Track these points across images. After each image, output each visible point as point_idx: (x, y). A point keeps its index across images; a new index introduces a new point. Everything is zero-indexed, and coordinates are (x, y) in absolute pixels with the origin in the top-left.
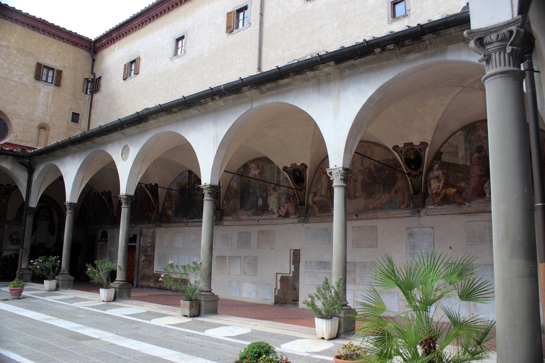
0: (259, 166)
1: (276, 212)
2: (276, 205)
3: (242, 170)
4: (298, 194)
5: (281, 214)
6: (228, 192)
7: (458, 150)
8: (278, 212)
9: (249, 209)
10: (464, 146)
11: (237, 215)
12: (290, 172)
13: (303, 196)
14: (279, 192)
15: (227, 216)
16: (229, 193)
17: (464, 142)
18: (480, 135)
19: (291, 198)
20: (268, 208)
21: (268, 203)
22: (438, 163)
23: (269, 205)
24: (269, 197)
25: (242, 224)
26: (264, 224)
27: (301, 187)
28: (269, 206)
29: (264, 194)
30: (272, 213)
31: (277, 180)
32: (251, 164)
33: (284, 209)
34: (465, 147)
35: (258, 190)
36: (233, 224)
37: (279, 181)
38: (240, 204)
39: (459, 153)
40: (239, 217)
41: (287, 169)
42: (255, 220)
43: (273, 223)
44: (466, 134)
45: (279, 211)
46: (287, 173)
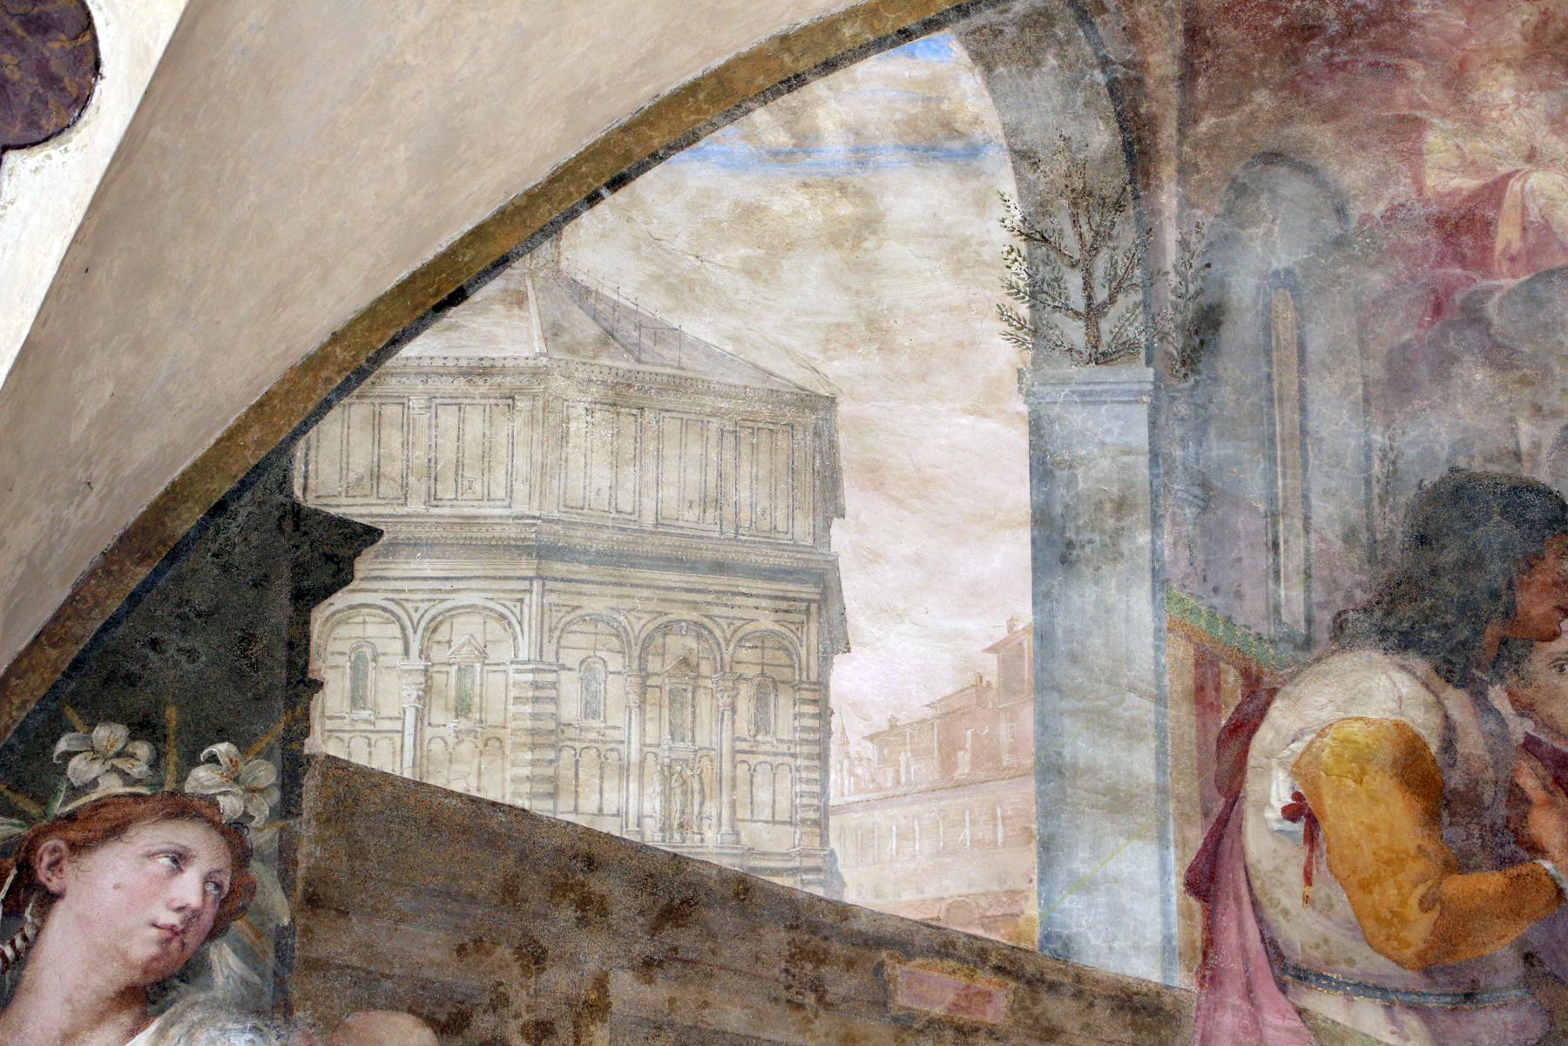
7: (828, 502)
10: (1018, 439)
17: (1036, 334)
18: (1495, 190)
22: (181, 808)
34: (1043, 468)
39: (855, 589)
44: (1101, 137)
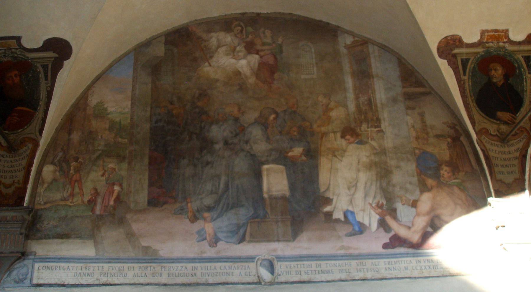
0: (258, 41)
1: (374, 225)
2: (366, 195)
3: (160, 50)
4: (491, 154)
5: (403, 232)
6: (70, 133)
8: (383, 224)
9: (209, 209)
11: (131, 236)
12: (465, 63)
13: (516, 162)
14: (373, 143)
15: (64, 236)
16: (76, 137)
19: (445, 171)
20: (328, 209)
21: (322, 189)
23: (329, 195)
24: (324, 163)
25: (164, 279)
26: (305, 278)
27: (504, 128)
28: (328, 201)
29: (297, 151)
30: (348, 229)
31: (357, 98)
32: (209, 31)
33: (418, 215)
35: (256, 132)
36: (104, 280)
37: (370, 103)
38: (151, 184)
40: (144, 243)
41: (456, 51)
42: (250, 259)
43: (361, 275)
45: (389, 220)
46: (453, 64)
